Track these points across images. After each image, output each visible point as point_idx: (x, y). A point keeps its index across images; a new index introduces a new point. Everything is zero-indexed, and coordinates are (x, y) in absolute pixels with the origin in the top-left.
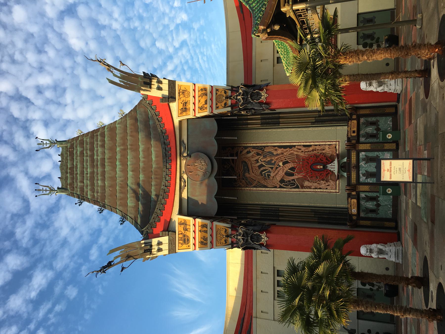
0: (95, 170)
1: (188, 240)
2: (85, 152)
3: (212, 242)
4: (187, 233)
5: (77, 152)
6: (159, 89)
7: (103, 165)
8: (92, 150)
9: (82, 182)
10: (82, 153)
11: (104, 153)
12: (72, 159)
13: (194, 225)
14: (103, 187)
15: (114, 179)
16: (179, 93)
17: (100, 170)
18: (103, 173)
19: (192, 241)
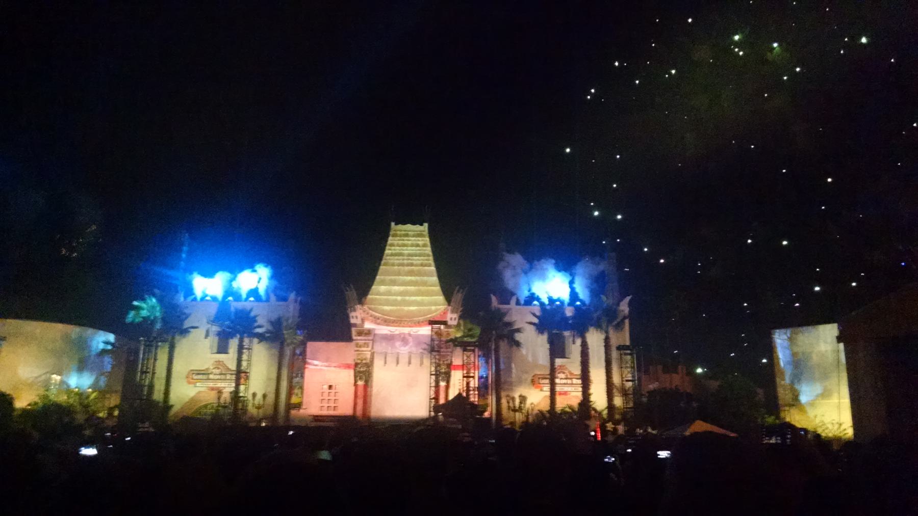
0: (405, 258)
1: (359, 336)
2: (418, 248)
3: (357, 351)
4: (363, 335)
5: (419, 240)
6: (451, 319)
7: (408, 265)
8: (420, 255)
9: (398, 245)
10: (418, 245)
11: (416, 265)
12: (414, 236)
13: (369, 340)
14: (393, 265)
15: (399, 274)
16: (448, 331)
17: (405, 262)
18: (403, 265)
19: (359, 338)
